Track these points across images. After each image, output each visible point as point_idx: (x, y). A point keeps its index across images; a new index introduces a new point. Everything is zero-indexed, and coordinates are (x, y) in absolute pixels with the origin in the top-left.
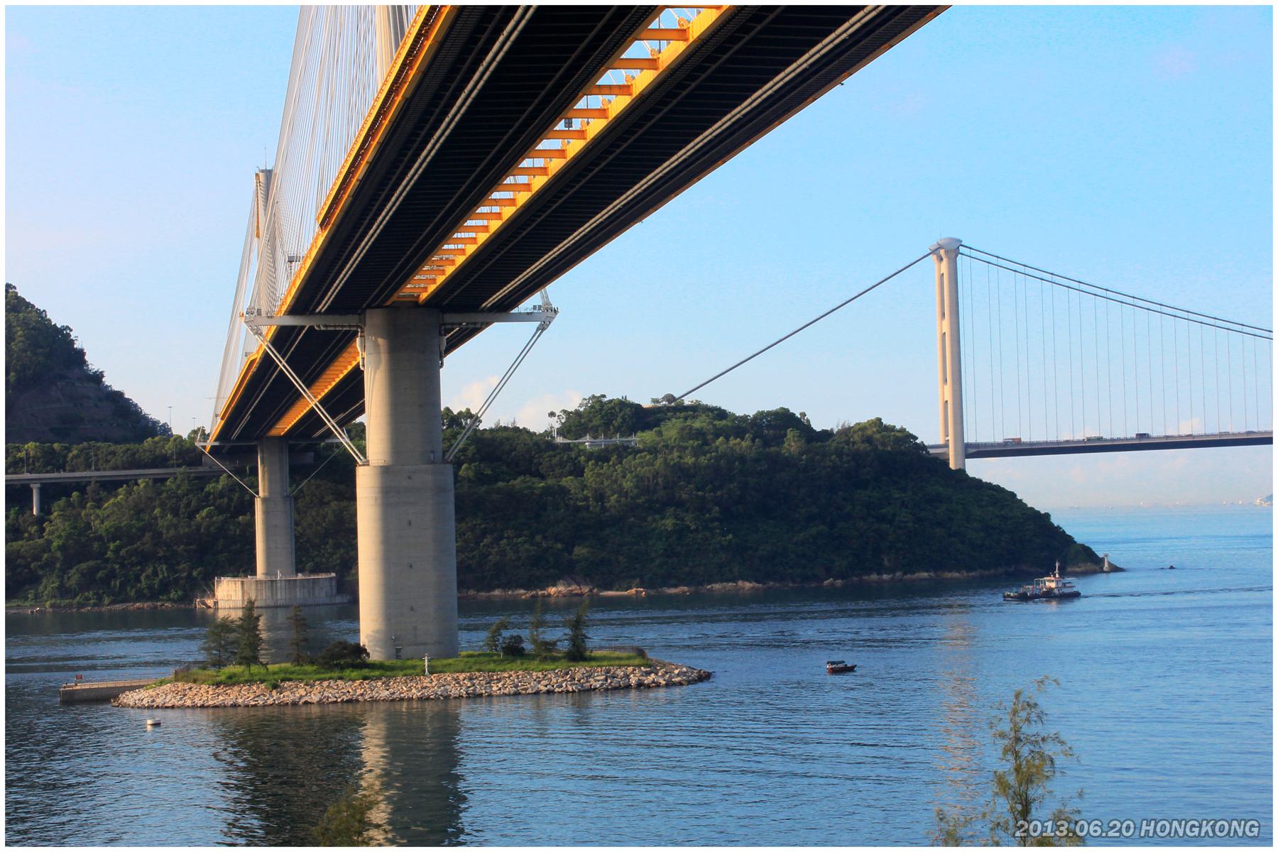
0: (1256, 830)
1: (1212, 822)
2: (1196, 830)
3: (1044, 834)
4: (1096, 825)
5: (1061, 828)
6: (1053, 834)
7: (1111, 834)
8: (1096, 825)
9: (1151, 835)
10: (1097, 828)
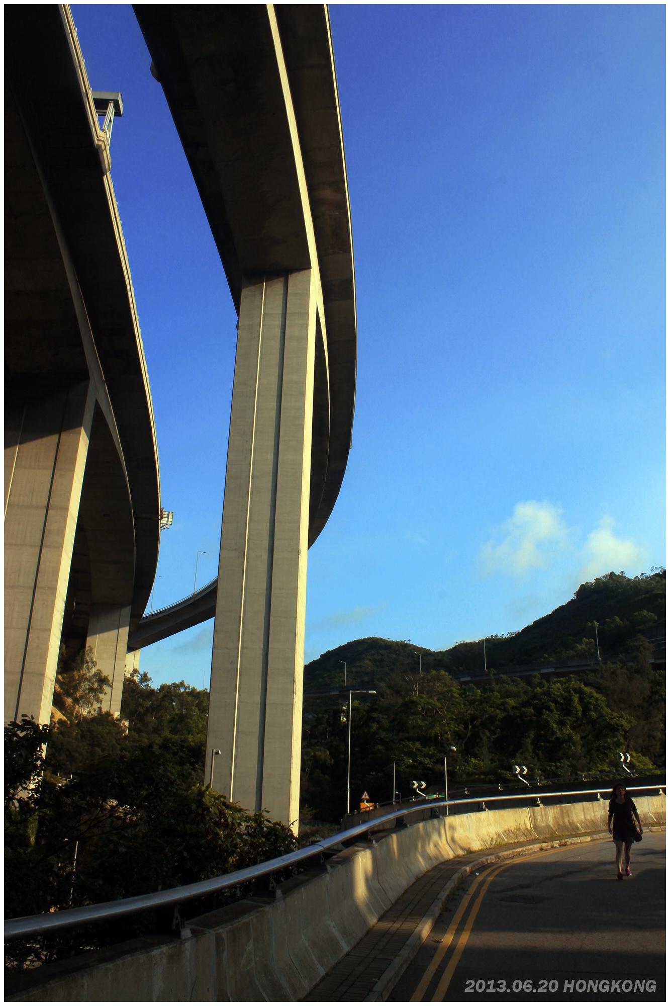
0: (654, 988)
1: (620, 981)
2: (607, 987)
3: (488, 991)
4: (528, 983)
5: (501, 986)
6: (494, 991)
7: (540, 990)
8: (528, 983)
9: (571, 991)
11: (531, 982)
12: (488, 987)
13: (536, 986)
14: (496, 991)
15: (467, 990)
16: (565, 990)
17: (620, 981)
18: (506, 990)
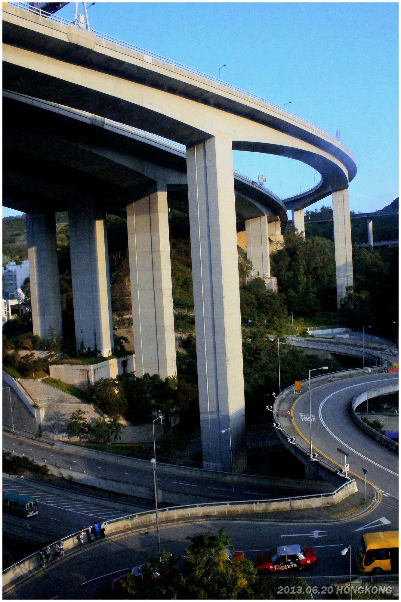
1: (370, 587)
2: (363, 591)
3: (291, 593)
4: (315, 588)
5: (299, 590)
6: (295, 593)
7: (322, 593)
8: (315, 588)
10: (315, 590)
11: (317, 588)
12: (291, 590)
13: (320, 590)
14: (296, 593)
15: (278, 593)
16: (337, 593)
17: (370, 587)
18: (302, 593)
